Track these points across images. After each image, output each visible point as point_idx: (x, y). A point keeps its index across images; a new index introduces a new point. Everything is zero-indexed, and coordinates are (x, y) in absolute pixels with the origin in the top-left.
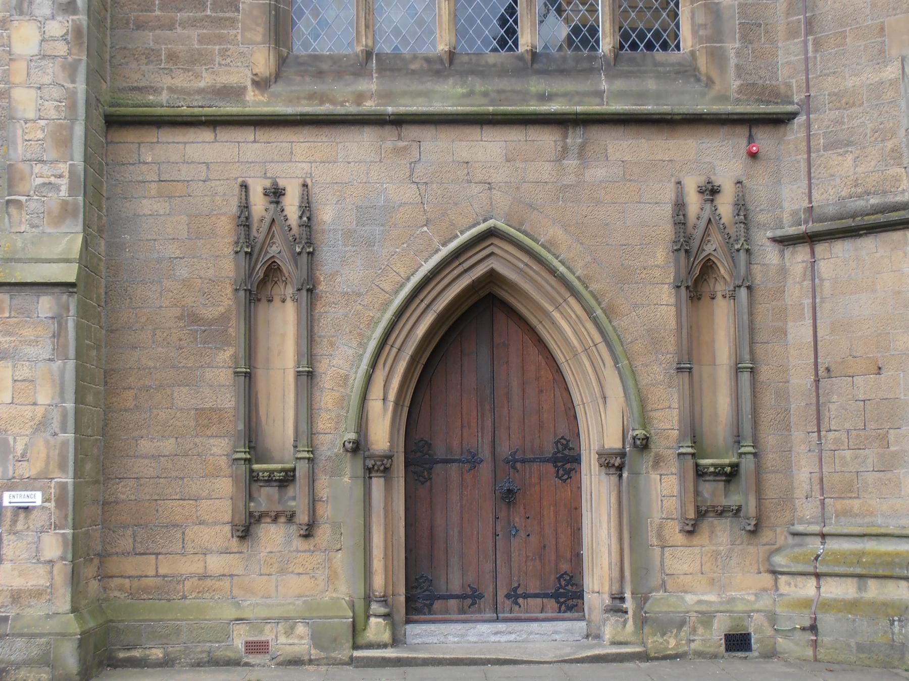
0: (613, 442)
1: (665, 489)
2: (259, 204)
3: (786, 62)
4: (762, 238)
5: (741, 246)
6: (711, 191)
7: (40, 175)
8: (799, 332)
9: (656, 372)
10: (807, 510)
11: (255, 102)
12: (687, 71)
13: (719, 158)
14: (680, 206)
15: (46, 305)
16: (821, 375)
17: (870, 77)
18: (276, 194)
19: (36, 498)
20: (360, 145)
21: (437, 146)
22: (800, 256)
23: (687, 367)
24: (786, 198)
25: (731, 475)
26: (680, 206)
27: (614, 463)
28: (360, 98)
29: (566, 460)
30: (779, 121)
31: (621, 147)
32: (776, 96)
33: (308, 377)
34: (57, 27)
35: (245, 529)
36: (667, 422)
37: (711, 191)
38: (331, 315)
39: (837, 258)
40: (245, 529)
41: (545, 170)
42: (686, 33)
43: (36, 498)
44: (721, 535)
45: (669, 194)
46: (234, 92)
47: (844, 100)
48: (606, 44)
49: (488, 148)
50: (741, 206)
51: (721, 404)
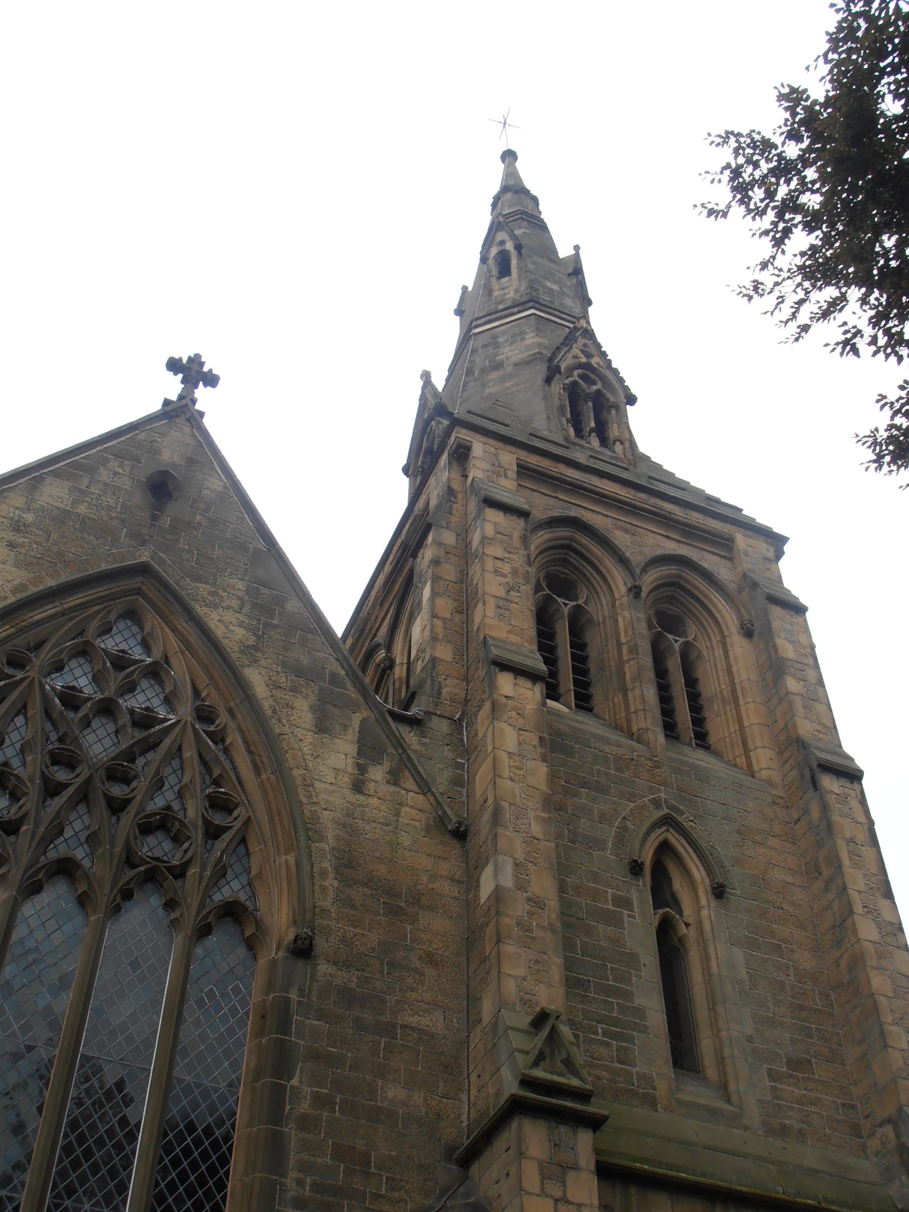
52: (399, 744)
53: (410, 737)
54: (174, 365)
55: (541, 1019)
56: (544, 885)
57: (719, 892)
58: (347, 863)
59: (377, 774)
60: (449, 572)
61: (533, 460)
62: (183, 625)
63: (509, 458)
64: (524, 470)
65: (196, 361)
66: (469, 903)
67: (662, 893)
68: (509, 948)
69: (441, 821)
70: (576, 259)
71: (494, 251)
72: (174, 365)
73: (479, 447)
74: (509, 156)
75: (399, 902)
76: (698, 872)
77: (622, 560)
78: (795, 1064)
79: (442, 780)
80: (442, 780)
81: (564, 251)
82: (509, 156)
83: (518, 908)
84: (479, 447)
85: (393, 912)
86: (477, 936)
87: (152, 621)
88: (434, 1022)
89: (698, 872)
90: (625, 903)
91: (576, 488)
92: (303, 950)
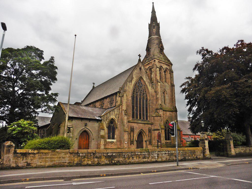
0: (146, 140)
1: (148, 143)
2: (131, 127)
3: (153, 121)
4: (152, 130)
5: (151, 131)
6: (150, 127)
7: (126, 125)
8: (153, 135)
9: (148, 136)
10: (154, 144)
11: (131, 121)
12: (149, 121)
13: (150, 126)
14: (149, 128)
15: (127, 132)
16: (154, 137)
17: (157, 123)
18: (132, 126)
19: (126, 142)
20: (136, 124)
21: (139, 124)
22: (153, 131)
23: (149, 136)
24: (153, 128)
25: (151, 142)
26: (149, 128)
27: (145, 141)
28: (136, 121)
29: (142, 141)
30: (152, 124)
31: (146, 125)
32: (153, 123)
33: (133, 136)
34: (126, 117)
35: (131, 144)
36: (148, 139)
37: (150, 127)
38: (135, 133)
39: (155, 131)
40: (131, 144)
41: (143, 126)
42: (148, 119)
43: (126, 142)
44: (150, 145)
45: (148, 127)
46: (130, 120)
47: (156, 124)
48: (145, 119)
49: (141, 125)
50: (151, 128)
51: (150, 138)
52: (153, 86)
53: (153, 86)
54: (139, 55)
55: (161, 104)
56: (160, 96)
57: (167, 94)
58: (151, 95)
59: (152, 89)
60: (154, 72)
61: (159, 61)
62: (143, 80)
63: (158, 61)
64: (159, 62)
65: (140, 55)
66: (156, 97)
67: (164, 94)
68: (159, 100)
69: (155, 91)
70: (159, 23)
71: (153, 25)
72: (139, 55)
73: (156, 60)
74: (153, 3)
75: (153, 97)
76: (166, 92)
77: (163, 69)
78: (169, 103)
79: (155, 88)
80: (155, 88)
81: (158, 22)
82: (153, 3)
83: (159, 98)
84: (156, 60)
85: (153, 97)
86: (157, 99)
87: (141, 80)
88: (155, 103)
89: (166, 92)
90: (162, 95)
91: (161, 63)
92: (150, 100)
